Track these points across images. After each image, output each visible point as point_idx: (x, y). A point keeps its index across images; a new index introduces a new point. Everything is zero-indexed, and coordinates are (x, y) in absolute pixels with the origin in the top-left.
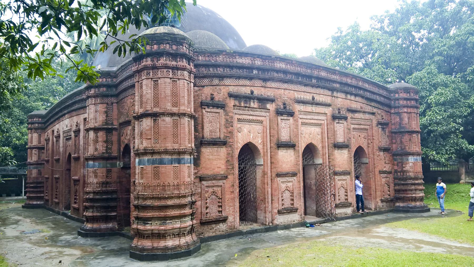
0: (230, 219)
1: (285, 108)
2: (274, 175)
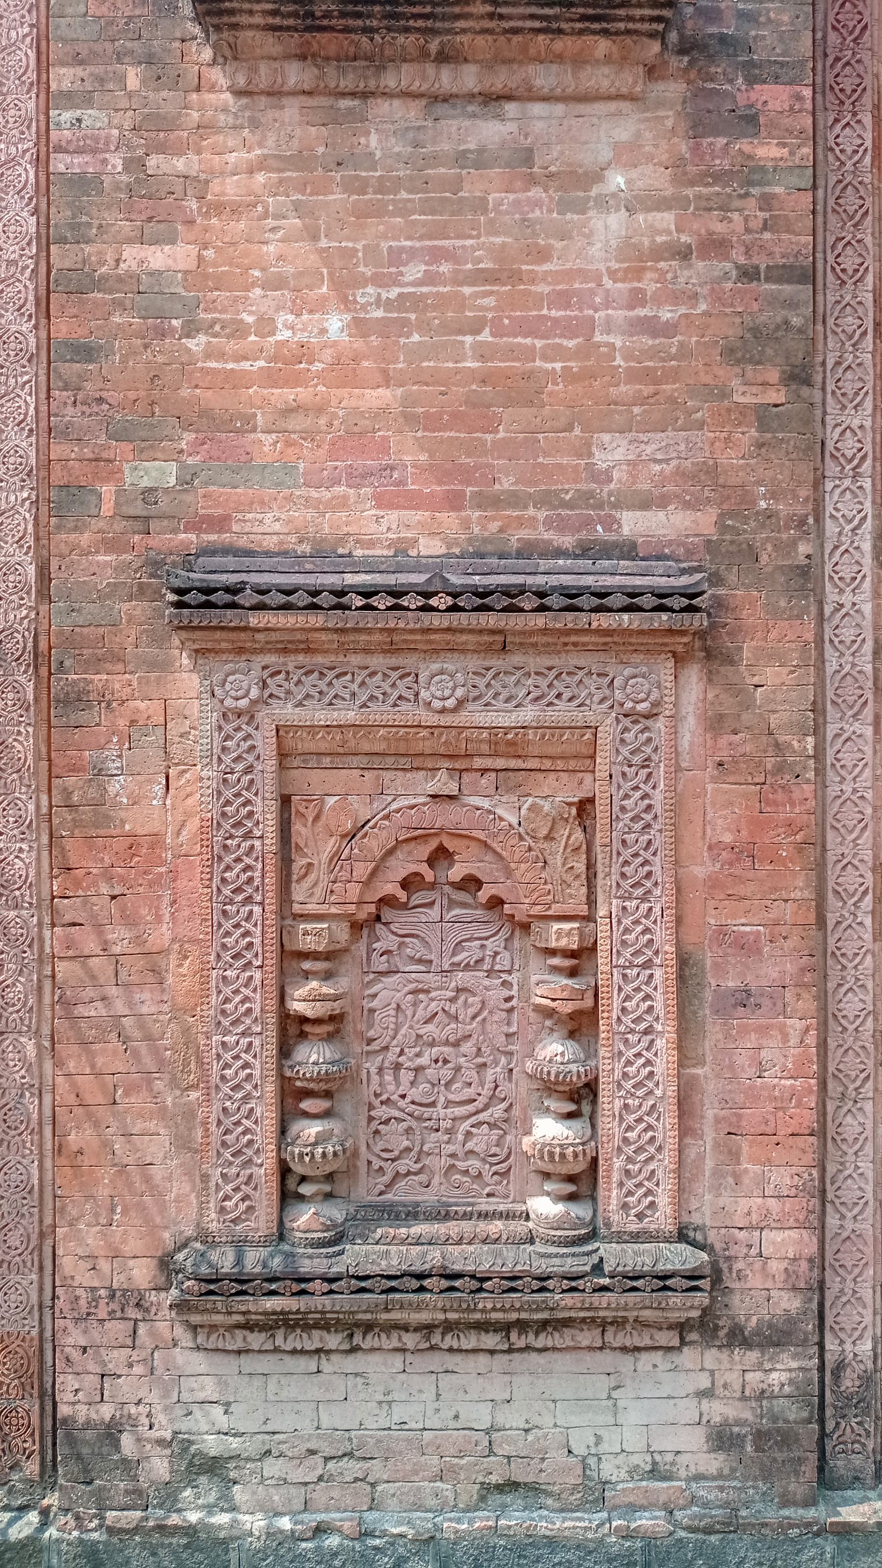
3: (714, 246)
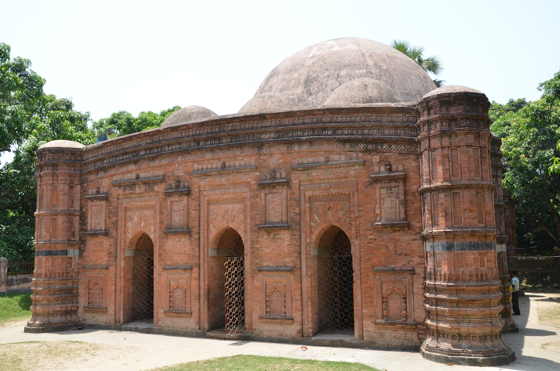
0: (111, 310)
1: (178, 187)
2: (161, 269)
3: (293, 244)
